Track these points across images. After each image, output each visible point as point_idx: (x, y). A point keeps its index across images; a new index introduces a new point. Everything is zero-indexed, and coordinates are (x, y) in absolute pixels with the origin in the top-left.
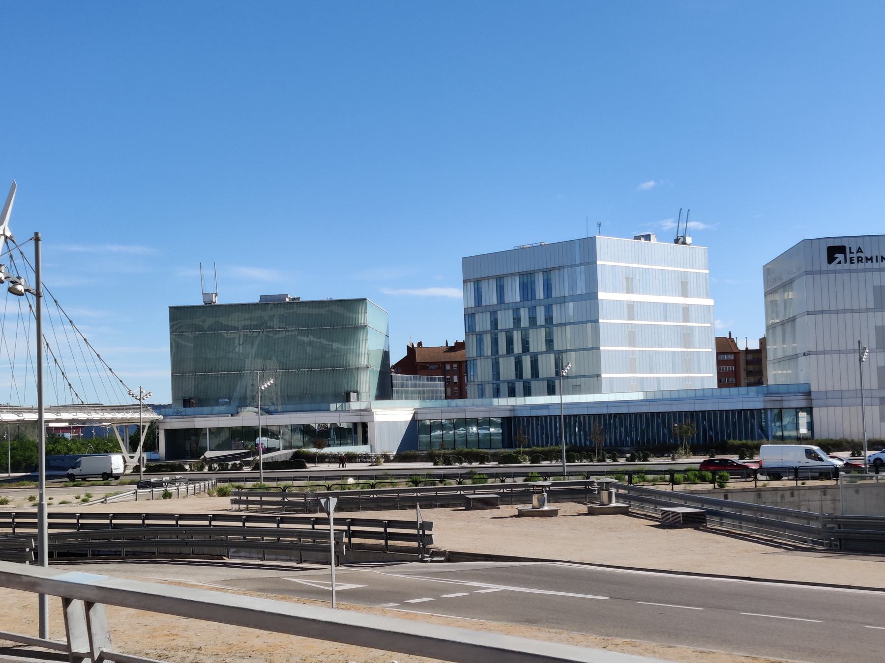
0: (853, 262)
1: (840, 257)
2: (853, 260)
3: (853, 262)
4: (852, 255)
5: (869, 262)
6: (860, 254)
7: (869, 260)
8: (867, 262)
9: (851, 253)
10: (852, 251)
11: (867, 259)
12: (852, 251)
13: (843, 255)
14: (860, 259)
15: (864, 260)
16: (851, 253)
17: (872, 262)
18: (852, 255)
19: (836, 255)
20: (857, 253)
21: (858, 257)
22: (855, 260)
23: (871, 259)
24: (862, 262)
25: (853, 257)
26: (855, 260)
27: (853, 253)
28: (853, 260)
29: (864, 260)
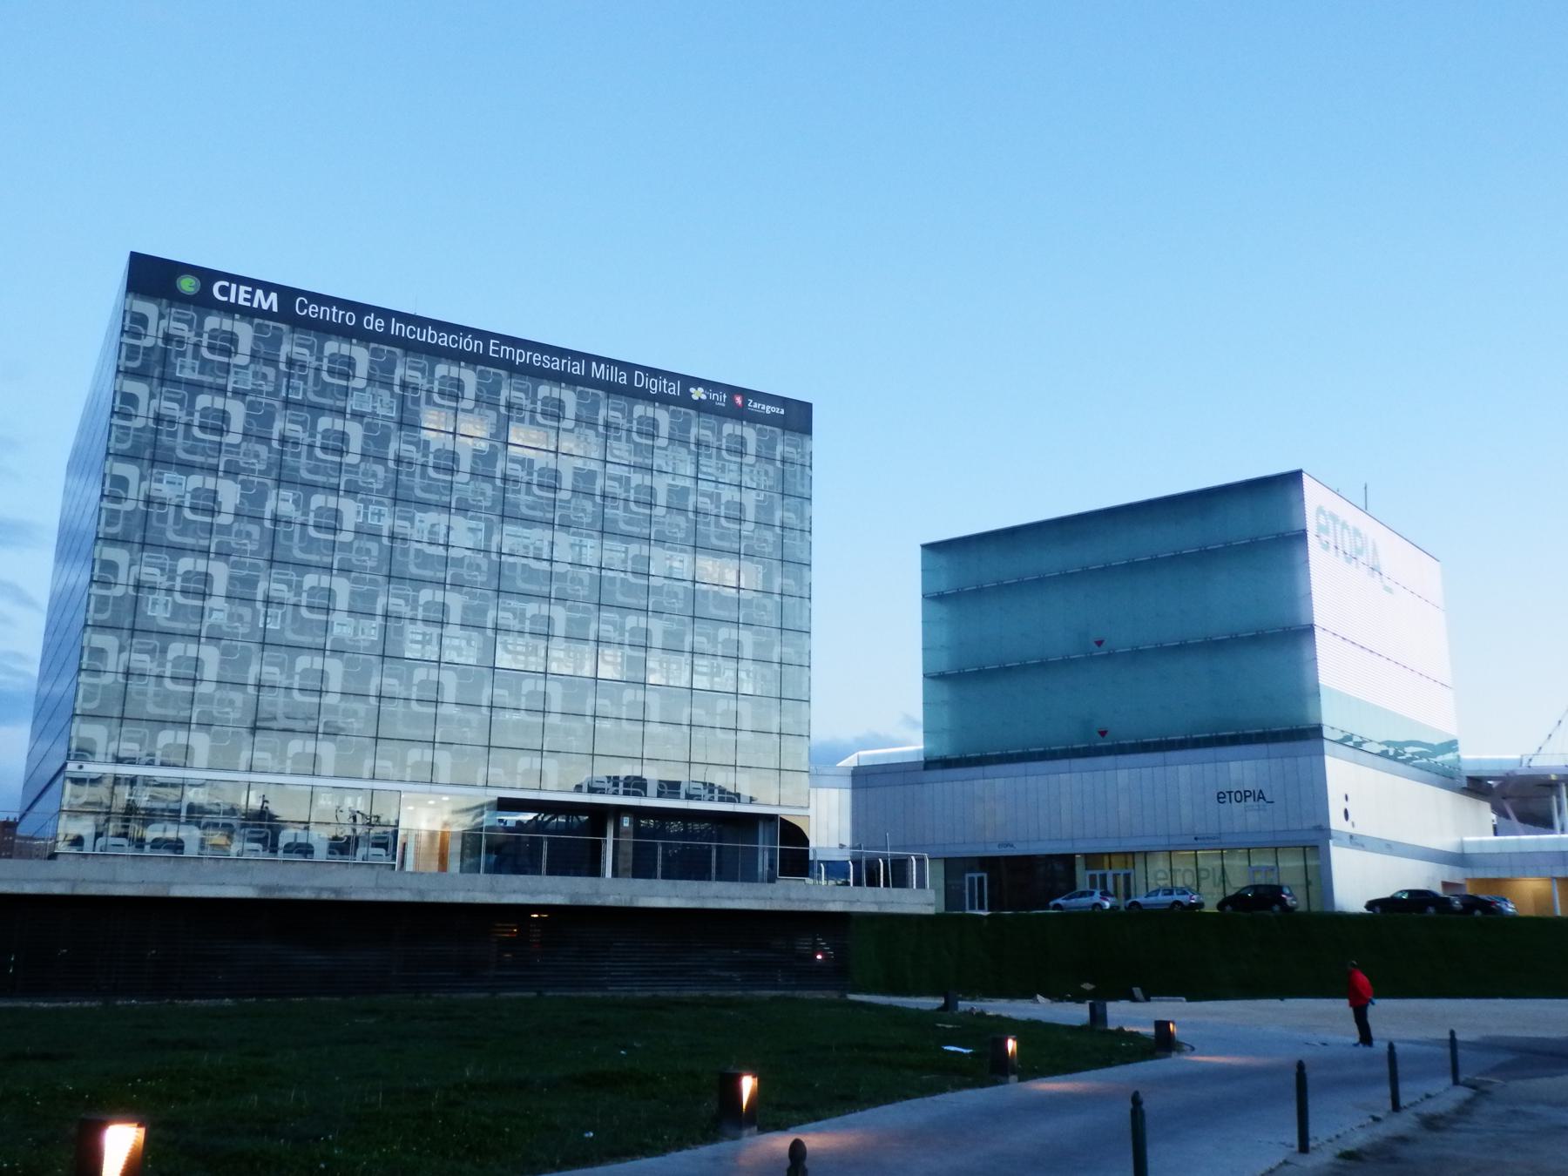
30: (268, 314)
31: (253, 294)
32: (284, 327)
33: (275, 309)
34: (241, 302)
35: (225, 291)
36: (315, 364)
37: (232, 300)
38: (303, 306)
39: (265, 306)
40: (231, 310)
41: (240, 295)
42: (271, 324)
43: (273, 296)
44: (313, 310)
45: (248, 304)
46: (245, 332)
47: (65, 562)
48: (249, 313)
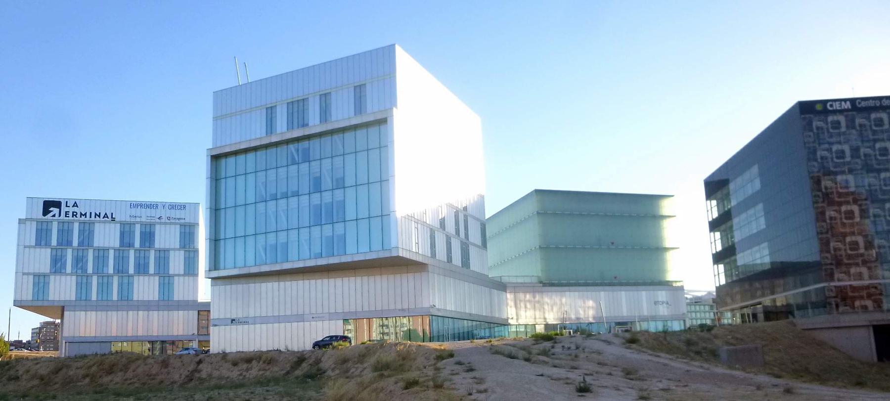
0: (67, 215)
1: (55, 211)
2: (68, 214)
3: (67, 215)
4: (67, 209)
5: (83, 217)
6: (75, 209)
7: (83, 215)
8: (81, 217)
9: (67, 206)
10: (68, 205)
11: (81, 214)
12: (68, 205)
13: (58, 209)
14: (75, 214)
15: (78, 215)
16: (67, 206)
17: (86, 217)
18: (67, 209)
19: (51, 209)
20: (73, 207)
21: (73, 212)
22: (71, 214)
23: (85, 214)
24: (76, 217)
25: (68, 212)
26: (71, 214)
27: (69, 207)
28: (68, 214)
29: (78, 215)
30: (847, 110)
31: (841, 104)
32: (854, 113)
33: (850, 107)
34: (838, 108)
35: (831, 106)
36: (869, 124)
37: (835, 108)
38: (859, 103)
39: (846, 107)
40: (835, 112)
41: (837, 106)
42: (850, 113)
43: (848, 103)
44: (863, 104)
45: (840, 108)
46: (841, 118)
47: (459, 333)
48: (841, 112)
